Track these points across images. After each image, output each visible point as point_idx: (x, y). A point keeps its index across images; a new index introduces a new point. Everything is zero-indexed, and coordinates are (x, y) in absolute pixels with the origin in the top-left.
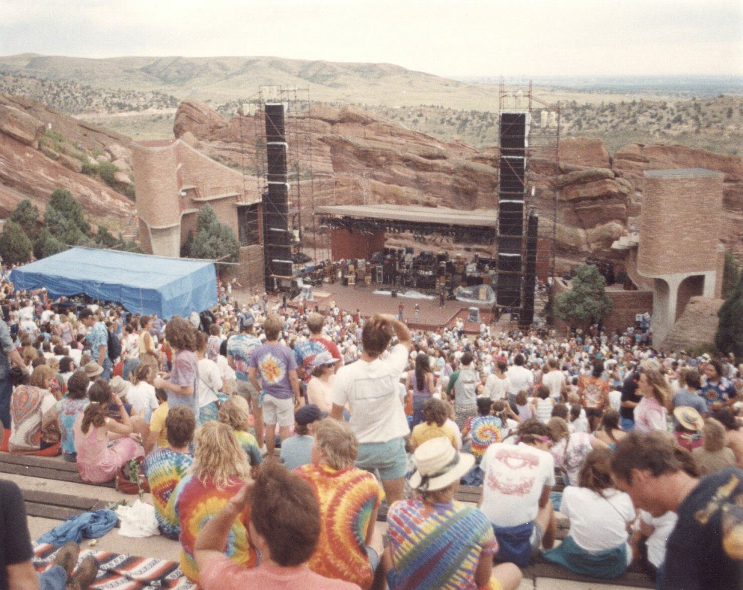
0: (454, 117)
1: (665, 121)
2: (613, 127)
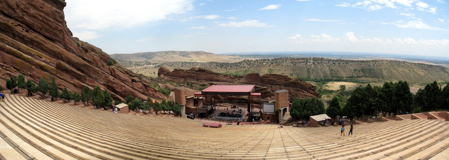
0: (219, 64)
1: (269, 64)
2: (258, 65)
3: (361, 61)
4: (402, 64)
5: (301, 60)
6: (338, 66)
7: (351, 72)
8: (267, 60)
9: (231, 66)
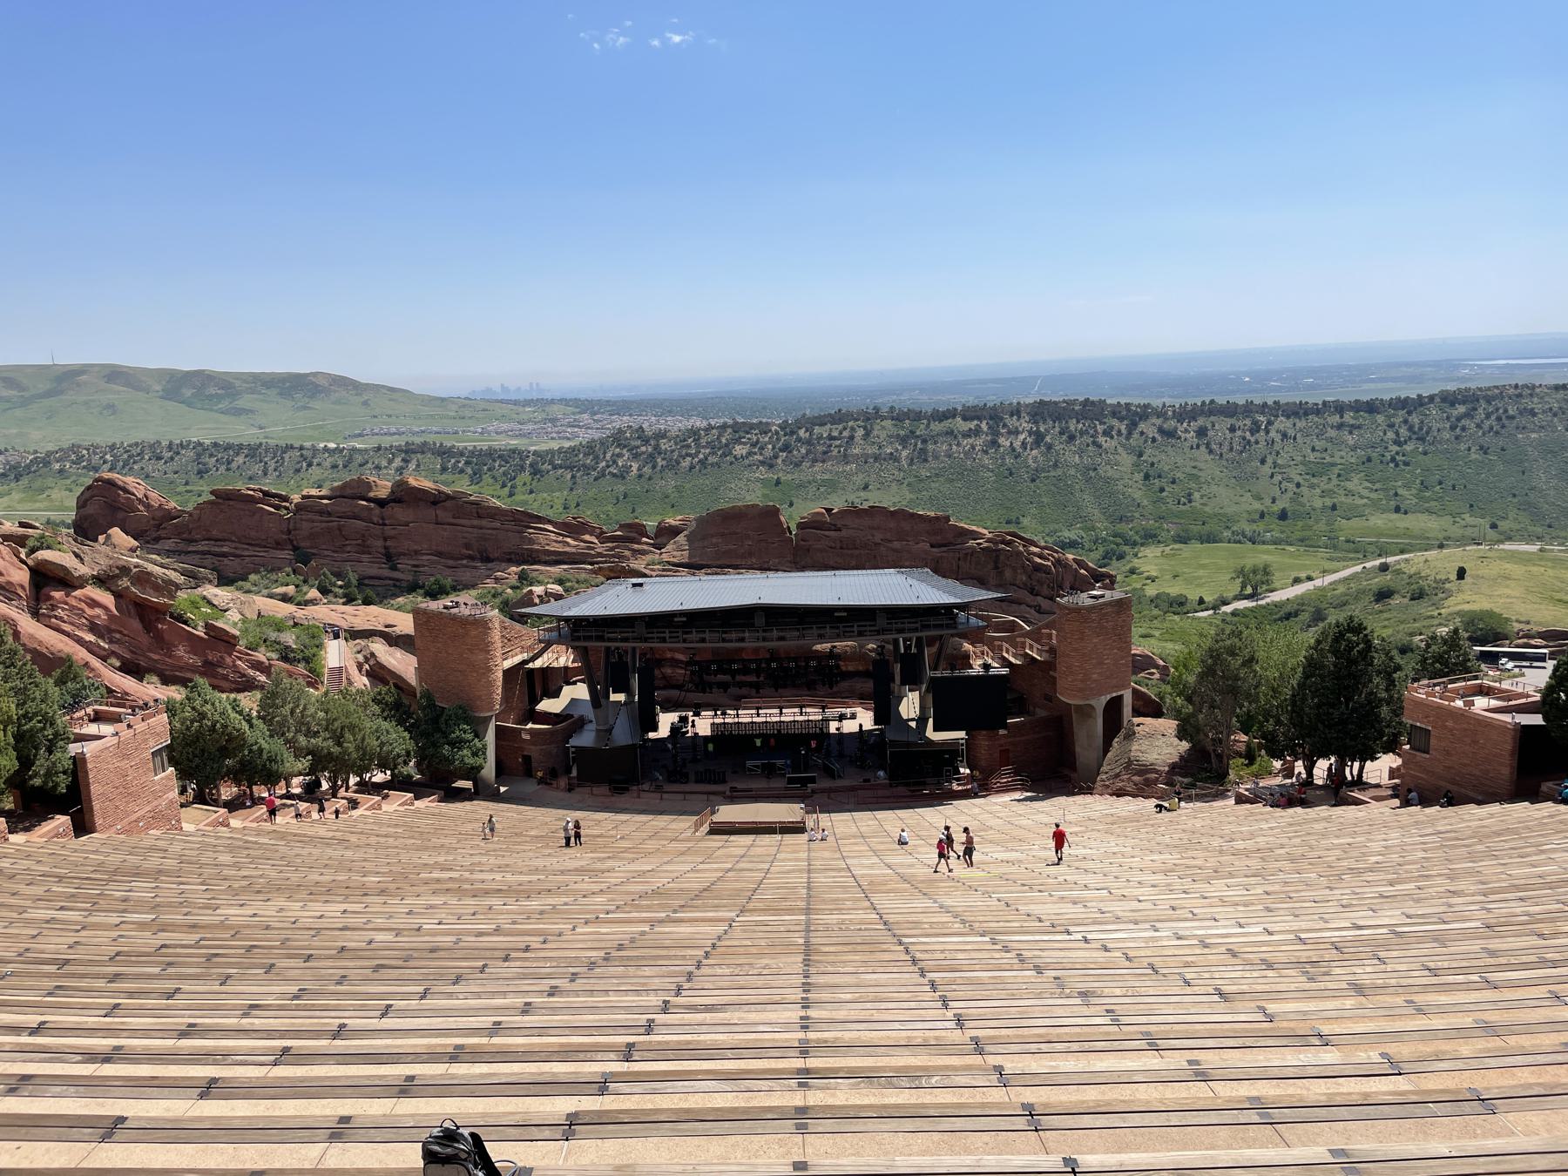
3: (1357, 407)
6: (1198, 447)
7: (1289, 480)
8: (752, 426)
9: (536, 472)
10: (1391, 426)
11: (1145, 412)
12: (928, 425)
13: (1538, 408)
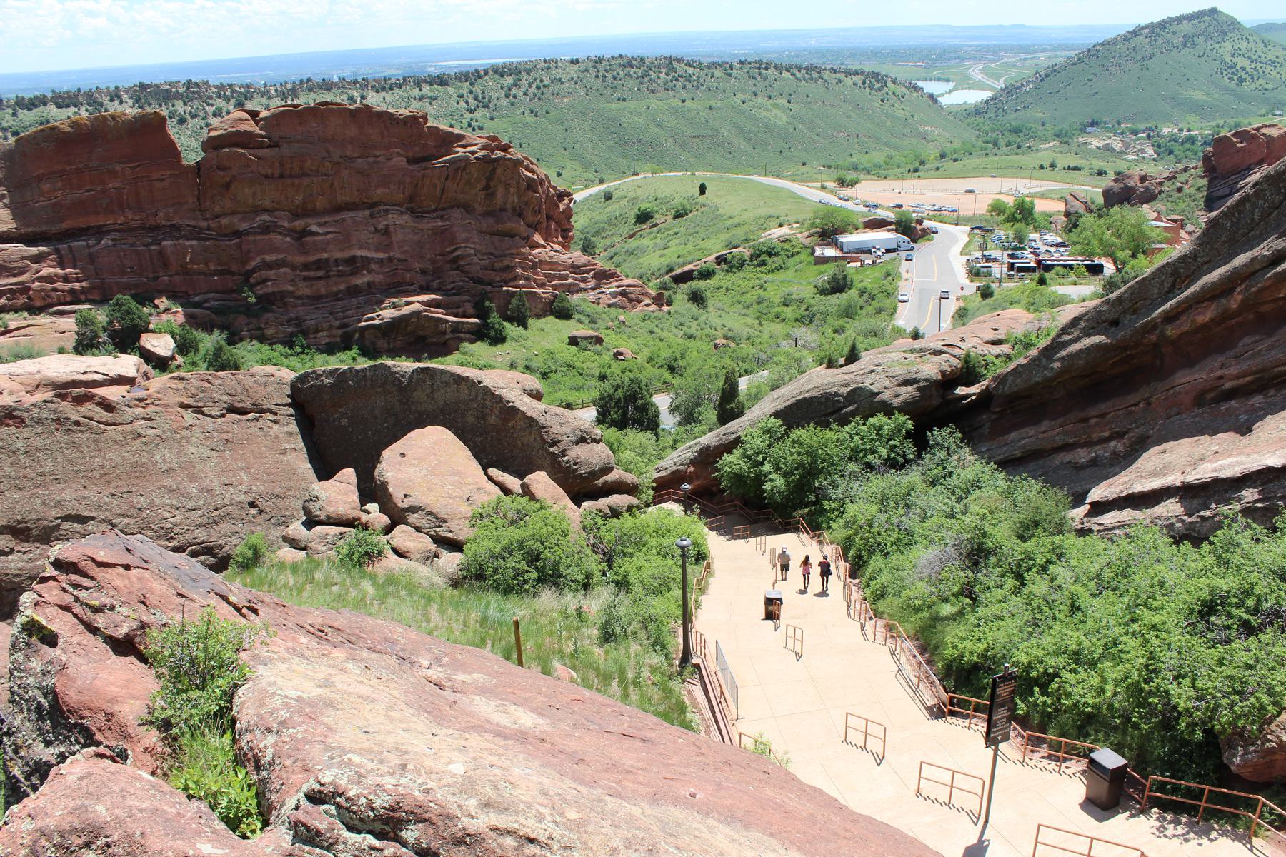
4: (663, 75)
5: (52, 107)
10: (461, 96)
11: (249, 92)
12: (14, 114)
13: (564, 78)
